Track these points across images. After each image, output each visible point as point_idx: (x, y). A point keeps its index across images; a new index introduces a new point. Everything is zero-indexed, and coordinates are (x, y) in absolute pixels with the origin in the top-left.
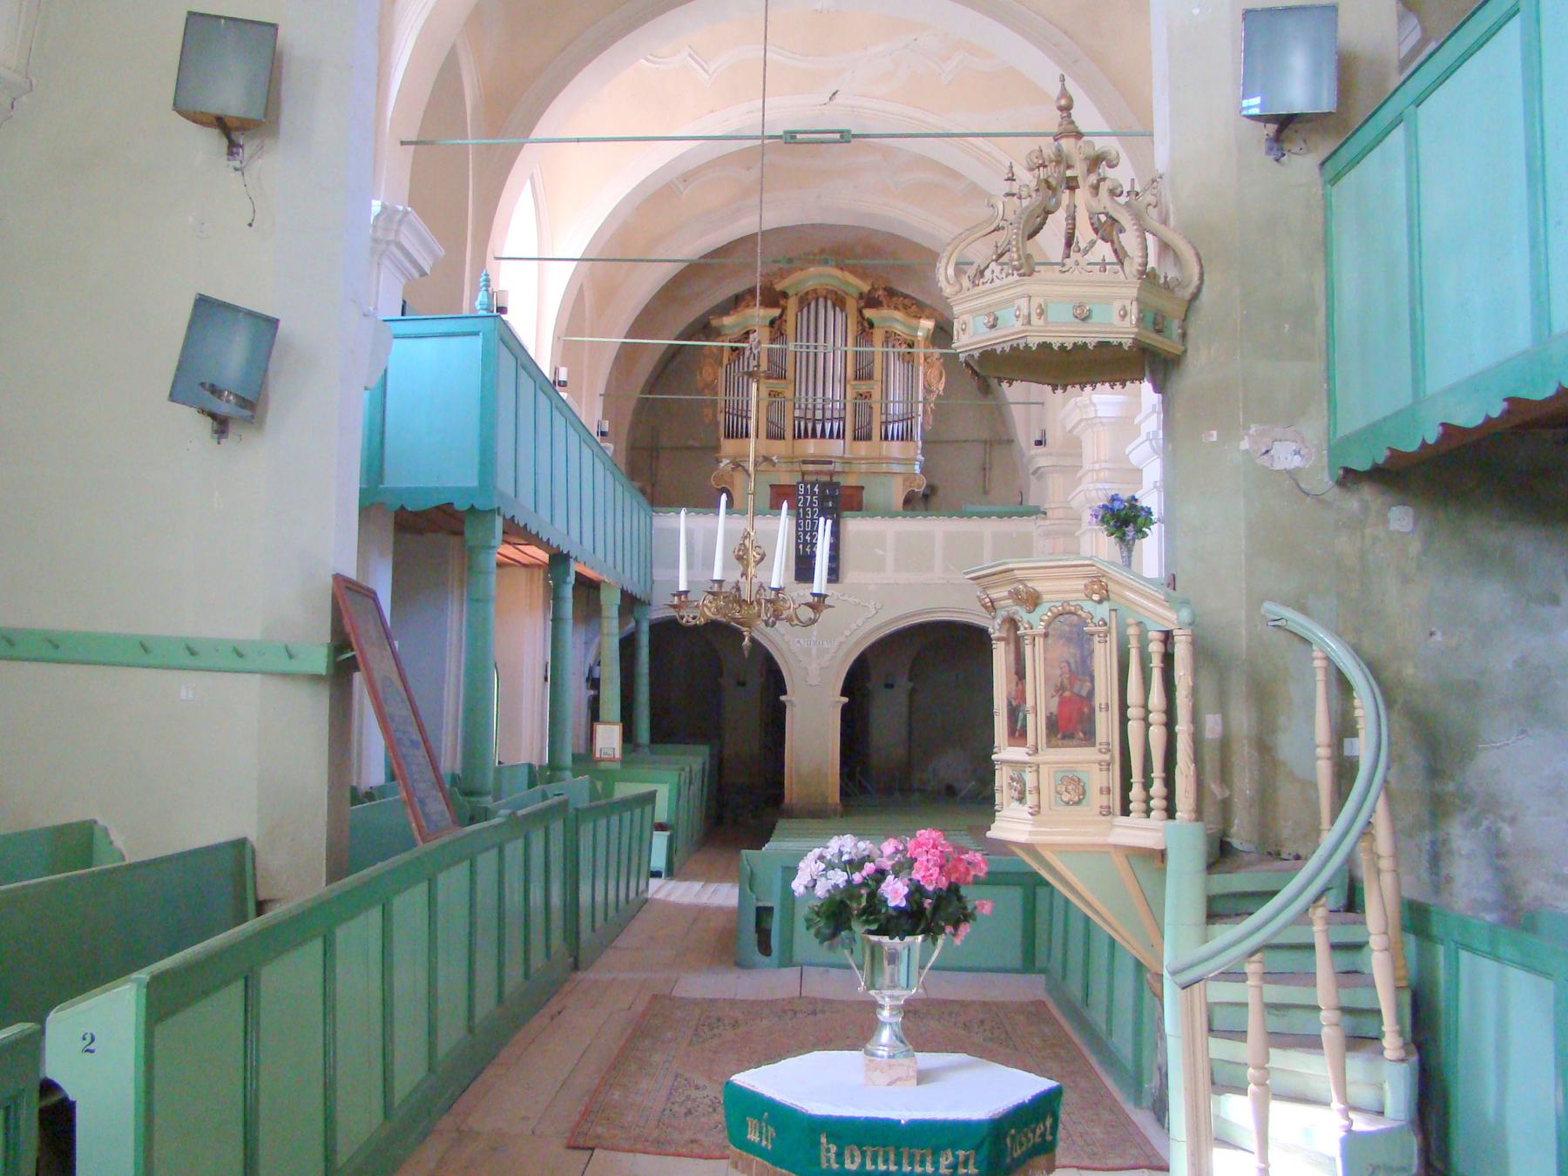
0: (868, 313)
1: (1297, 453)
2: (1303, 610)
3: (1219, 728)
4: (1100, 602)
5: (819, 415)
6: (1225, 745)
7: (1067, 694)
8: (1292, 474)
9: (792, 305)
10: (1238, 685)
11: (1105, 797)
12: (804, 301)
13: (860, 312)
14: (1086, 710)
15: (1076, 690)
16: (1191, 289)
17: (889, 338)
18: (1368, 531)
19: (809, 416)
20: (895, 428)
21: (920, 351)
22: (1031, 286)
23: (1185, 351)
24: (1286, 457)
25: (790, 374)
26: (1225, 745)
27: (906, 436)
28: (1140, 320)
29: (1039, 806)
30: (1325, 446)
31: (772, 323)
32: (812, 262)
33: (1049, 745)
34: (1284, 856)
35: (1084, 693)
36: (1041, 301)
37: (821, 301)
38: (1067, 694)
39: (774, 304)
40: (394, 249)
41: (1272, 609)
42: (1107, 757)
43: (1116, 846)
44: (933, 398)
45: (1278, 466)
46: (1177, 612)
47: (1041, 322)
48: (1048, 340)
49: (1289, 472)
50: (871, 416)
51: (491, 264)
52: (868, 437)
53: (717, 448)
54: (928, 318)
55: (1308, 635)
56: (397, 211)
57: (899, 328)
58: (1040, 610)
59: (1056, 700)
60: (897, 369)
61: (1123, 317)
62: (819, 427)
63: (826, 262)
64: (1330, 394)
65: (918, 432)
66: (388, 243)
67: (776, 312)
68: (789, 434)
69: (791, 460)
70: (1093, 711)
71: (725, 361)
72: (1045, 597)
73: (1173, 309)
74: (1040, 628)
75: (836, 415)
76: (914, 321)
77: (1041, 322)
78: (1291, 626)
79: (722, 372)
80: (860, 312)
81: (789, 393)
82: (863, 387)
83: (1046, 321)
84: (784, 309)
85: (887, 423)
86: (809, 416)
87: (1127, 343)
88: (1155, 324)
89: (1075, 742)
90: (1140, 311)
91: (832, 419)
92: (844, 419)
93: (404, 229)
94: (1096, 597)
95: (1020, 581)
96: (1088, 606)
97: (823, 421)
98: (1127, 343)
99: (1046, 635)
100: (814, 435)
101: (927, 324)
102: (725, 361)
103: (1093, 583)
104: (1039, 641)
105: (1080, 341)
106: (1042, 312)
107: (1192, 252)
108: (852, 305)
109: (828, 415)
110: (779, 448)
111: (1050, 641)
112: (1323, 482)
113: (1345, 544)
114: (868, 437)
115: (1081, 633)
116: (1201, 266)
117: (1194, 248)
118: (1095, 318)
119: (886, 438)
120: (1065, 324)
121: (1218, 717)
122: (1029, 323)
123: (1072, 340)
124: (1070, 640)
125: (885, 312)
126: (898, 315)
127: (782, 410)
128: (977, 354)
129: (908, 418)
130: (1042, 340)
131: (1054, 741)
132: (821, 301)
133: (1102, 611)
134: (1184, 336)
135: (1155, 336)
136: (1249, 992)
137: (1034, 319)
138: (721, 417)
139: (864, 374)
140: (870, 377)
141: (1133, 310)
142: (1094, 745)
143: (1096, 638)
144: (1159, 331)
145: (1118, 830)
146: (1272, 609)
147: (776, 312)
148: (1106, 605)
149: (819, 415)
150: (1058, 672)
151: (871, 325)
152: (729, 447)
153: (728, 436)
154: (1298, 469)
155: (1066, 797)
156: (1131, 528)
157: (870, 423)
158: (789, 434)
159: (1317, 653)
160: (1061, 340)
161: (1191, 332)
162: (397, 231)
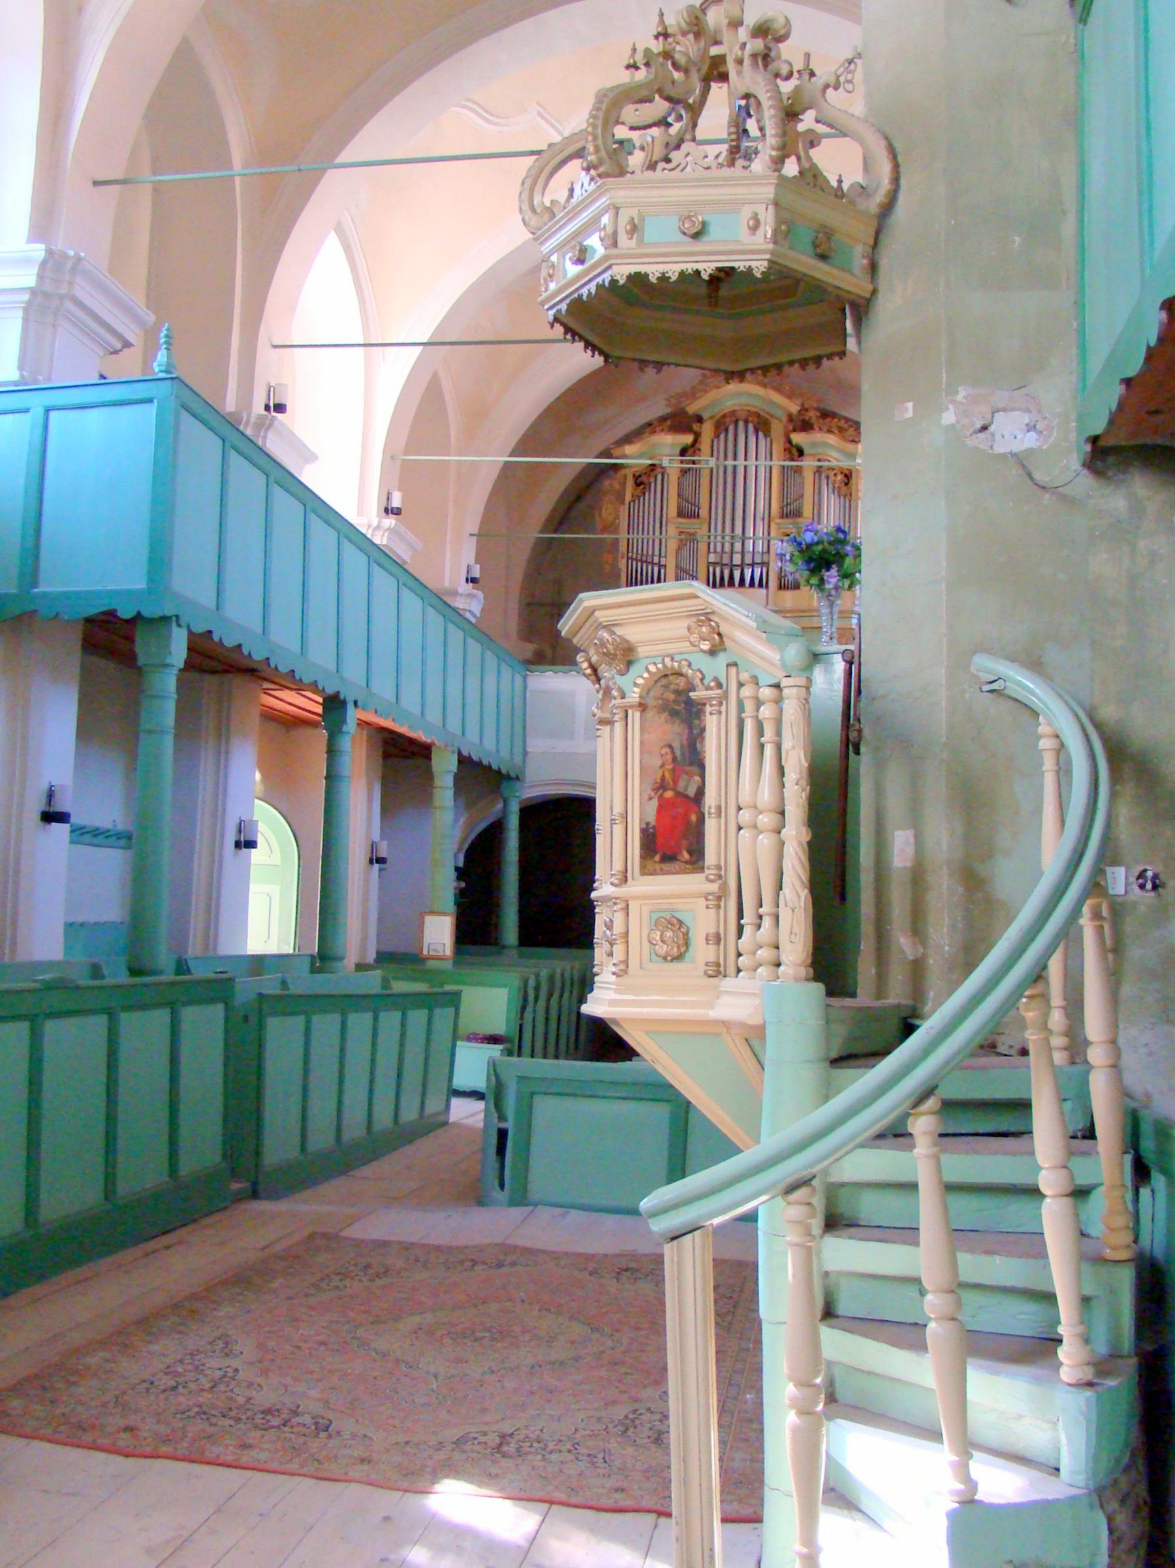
1: (1031, 428)
2: (1036, 666)
3: (910, 851)
4: (712, 652)
6: (918, 876)
7: (669, 794)
8: (1021, 461)
10: (936, 787)
11: (712, 948)
14: (694, 818)
15: (681, 786)
16: (880, 197)
18: (1142, 544)
22: (620, 192)
23: (874, 292)
24: (1013, 434)
25: (704, 513)
26: (918, 876)
28: (775, 232)
29: (626, 962)
30: (1073, 416)
33: (644, 871)
34: (1002, 1049)
35: (691, 791)
36: (634, 213)
38: (669, 794)
40: (69, 305)
41: (987, 665)
42: (714, 887)
43: (726, 1024)
45: (999, 449)
46: (781, 649)
47: (633, 243)
48: (642, 269)
49: (1014, 455)
51: (264, 353)
55: (1034, 701)
56: (65, 256)
58: (635, 670)
59: (654, 803)
61: (755, 227)
64: (1081, 332)
66: (62, 298)
70: (701, 820)
72: (642, 651)
73: (854, 233)
74: (634, 696)
77: (633, 243)
78: (1012, 690)
83: (641, 242)
87: (759, 266)
88: (815, 246)
89: (676, 866)
90: (779, 221)
93: (79, 280)
94: (705, 646)
95: (607, 627)
96: (702, 662)
98: (759, 266)
99: (642, 707)
103: (700, 623)
104: (635, 716)
105: (690, 268)
106: (634, 229)
107: (883, 143)
111: (650, 714)
112: (1069, 464)
113: (1103, 565)
115: (690, 703)
116: (896, 167)
117: (886, 138)
118: (715, 233)
120: (668, 244)
121: (910, 833)
122: (615, 244)
123: (678, 268)
124: (674, 714)
127: (694, 554)
128: (564, 307)
130: (633, 269)
131: (650, 865)
133: (716, 667)
134: (873, 267)
135: (813, 262)
136: (923, 1258)
137: (623, 239)
141: (768, 218)
142: (702, 869)
143: (708, 709)
144: (823, 257)
145: (724, 999)
146: (987, 665)
148: (722, 659)
150: (659, 762)
154: (1030, 451)
155: (663, 949)
156: (834, 571)
159: (1043, 729)
160: (661, 268)
161: (884, 263)
162: (71, 283)
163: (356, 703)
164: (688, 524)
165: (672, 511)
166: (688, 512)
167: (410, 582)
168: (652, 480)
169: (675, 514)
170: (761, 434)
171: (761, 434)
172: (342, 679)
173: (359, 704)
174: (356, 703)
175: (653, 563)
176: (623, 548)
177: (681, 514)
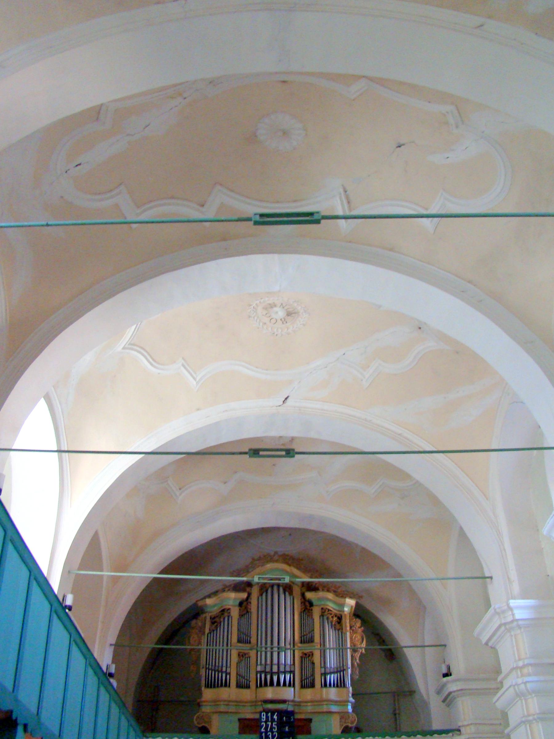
0: (309, 595)
5: (275, 669)
9: (255, 591)
12: (264, 588)
13: (303, 595)
17: (324, 612)
19: (268, 669)
20: (332, 678)
21: (347, 623)
25: (254, 640)
27: (340, 684)
31: (241, 604)
32: (268, 562)
37: (275, 588)
39: (244, 590)
44: (357, 655)
50: (313, 669)
52: (312, 685)
53: (201, 694)
54: (351, 598)
57: (331, 606)
60: (331, 635)
62: (275, 678)
63: (277, 561)
65: (348, 682)
67: (244, 595)
68: (253, 685)
69: (254, 703)
71: (207, 631)
75: (288, 669)
76: (340, 600)
79: (204, 640)
80: (303, 595)
81: (253, 653)
82: (307, 648)
84: (249, 595)
85: (325, 674)
86: (268, 669)
91: (285, 672)
92: (292, 672)
97: (278, 673)
100: (272, 684)
101: (351, 602)
102: (207, 631)
108: (297, 591)
109: (282, 669)
110: (247, 694)
114: (312, 685)
119: (325, 685)
125: (321, 594)
126: (330, 596)
127: (248, 667)
129: (341, 670)
132: (275, 588)
138: (203, 672)
139: (307, 639)
140: (311, 640)
147: (244, 595)
149: (275, 669)
151: (311, 604)
152: (208, 694)
153: (208, 686)
157: (313, 675)
158: (253, 685)
163: (25, 726)
164: (244, 647)
165: (235, 639)
166: (243, 639)
167: (79, 640)
168: (222, 620)
169: (236, 641)
170: (287, 593)
171: (287, 593)
172: (17, 700)
173: (29, 728)
174: (25, 726)
175: (222, 672)
176: (203, 661)
177: (239, 641)
